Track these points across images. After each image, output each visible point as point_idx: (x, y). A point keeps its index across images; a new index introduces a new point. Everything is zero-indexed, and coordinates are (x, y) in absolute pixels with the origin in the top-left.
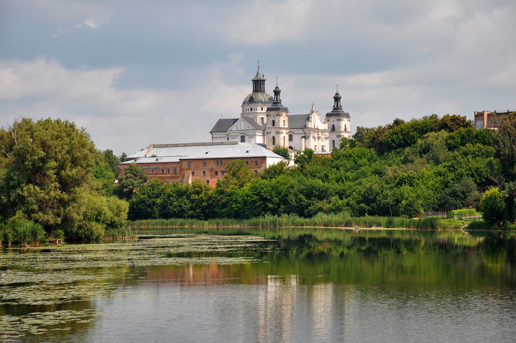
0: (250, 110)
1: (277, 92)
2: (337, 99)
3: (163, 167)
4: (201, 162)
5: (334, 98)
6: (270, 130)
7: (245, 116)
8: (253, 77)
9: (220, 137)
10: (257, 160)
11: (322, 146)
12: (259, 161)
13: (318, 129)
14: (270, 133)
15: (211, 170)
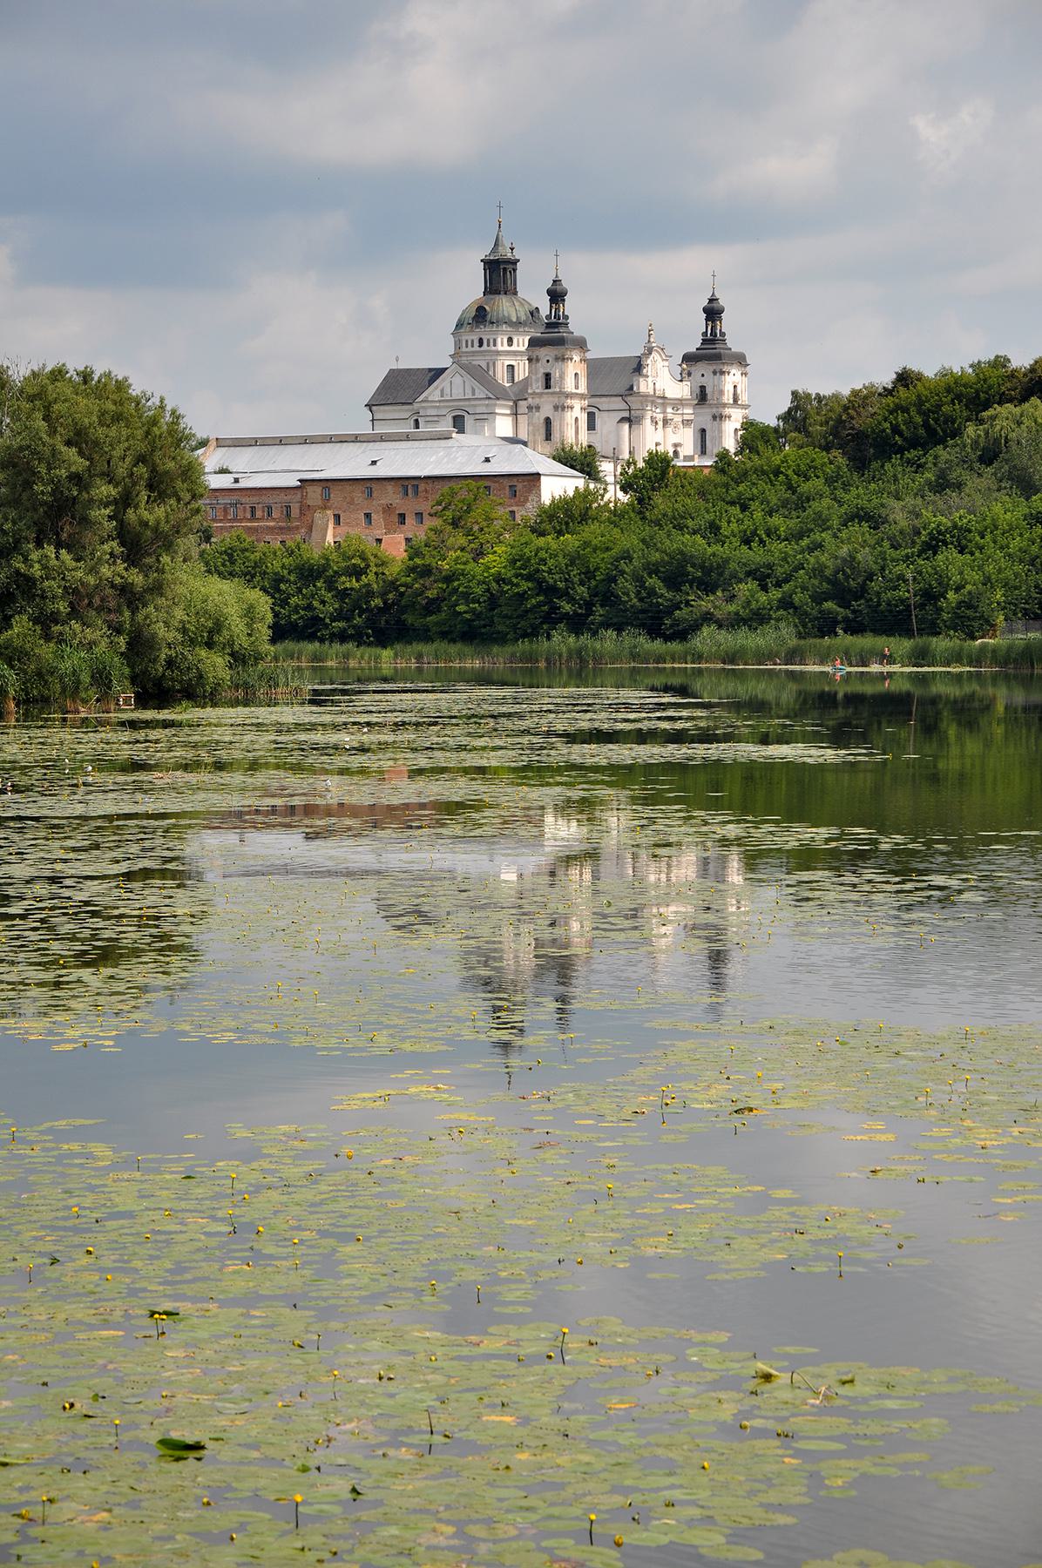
0: (476, 343)
2: (713, 313)
5: (705, 310)
7: (464, 360)
11: (676, 445)
14: (538, 408)
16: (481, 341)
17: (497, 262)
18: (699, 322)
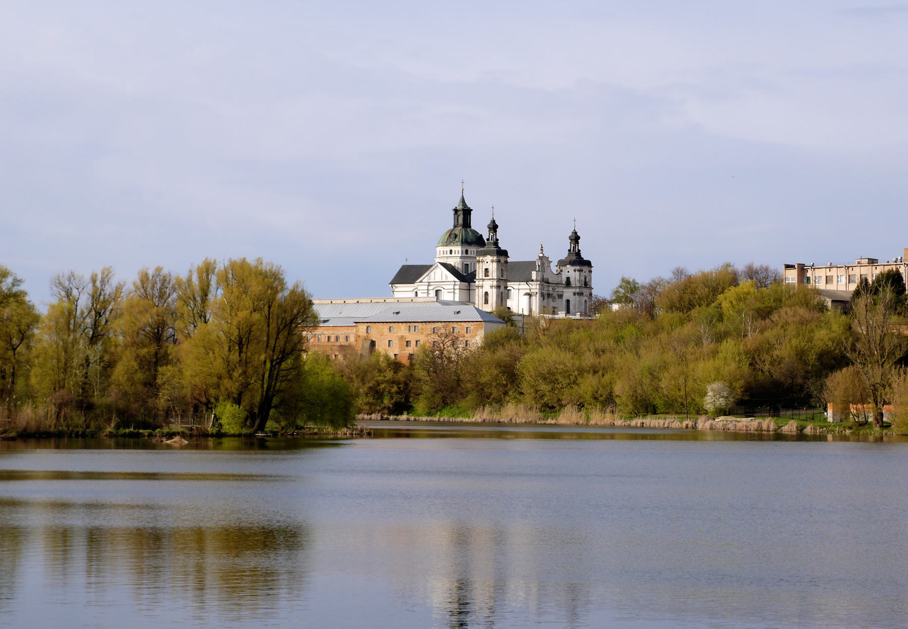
1: (494, 227)
2: (575, 239)
3: (331, 332)
4: (387, 326)
6: (481, 283)
12: (472, 328)
13: (548, 283)
15: (402, 337)
16: (451, 251)
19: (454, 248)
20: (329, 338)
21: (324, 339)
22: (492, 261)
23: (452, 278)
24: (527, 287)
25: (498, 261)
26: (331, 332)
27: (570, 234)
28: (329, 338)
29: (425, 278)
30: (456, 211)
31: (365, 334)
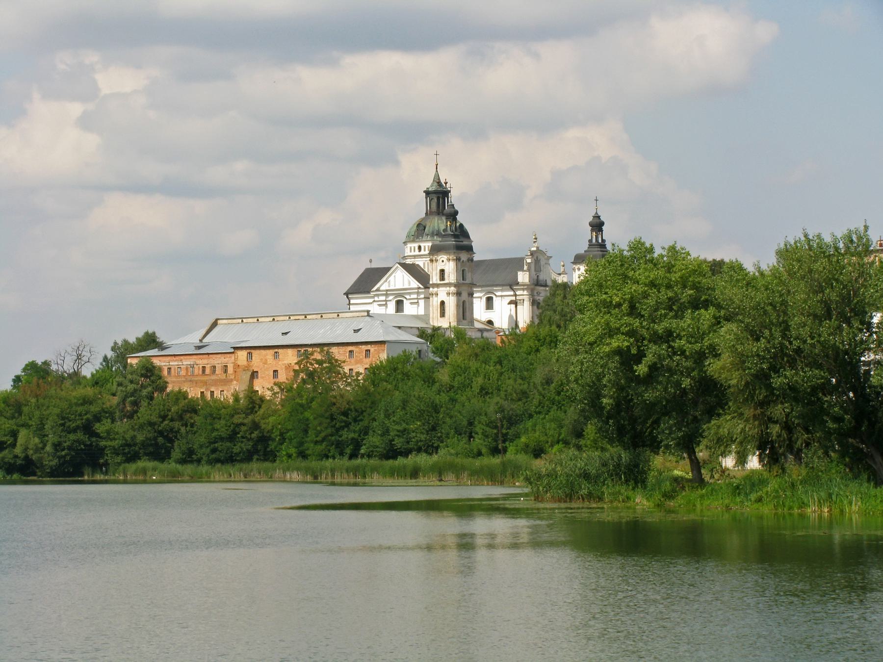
2: (597, 226)
3: (205, 361)
4: (272, 352)
5: (591, 224)
6: (436, 289)
7: (409, 261)
8: (428, 183)
9: (360, 303)
10: (369, 347)
12: (372, 350)
14: (437, 294)
16: (420, 248)
17: (435, 192)
18: (587, 233)
19: (422, 245)
20: (204, 368)
21: (198, 371)
22: (449, 260)
23: (415, 284)
24: (512, 293)
25: (458, 260)
26: (205, 361)
27: (591, 219)
28: (204, 368)
29: (383, 285)
30: (427, 193)
31: (245, 363)
